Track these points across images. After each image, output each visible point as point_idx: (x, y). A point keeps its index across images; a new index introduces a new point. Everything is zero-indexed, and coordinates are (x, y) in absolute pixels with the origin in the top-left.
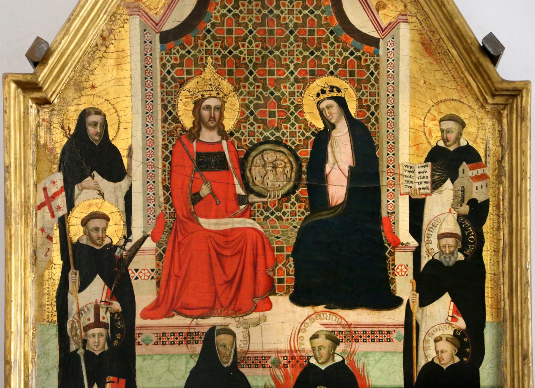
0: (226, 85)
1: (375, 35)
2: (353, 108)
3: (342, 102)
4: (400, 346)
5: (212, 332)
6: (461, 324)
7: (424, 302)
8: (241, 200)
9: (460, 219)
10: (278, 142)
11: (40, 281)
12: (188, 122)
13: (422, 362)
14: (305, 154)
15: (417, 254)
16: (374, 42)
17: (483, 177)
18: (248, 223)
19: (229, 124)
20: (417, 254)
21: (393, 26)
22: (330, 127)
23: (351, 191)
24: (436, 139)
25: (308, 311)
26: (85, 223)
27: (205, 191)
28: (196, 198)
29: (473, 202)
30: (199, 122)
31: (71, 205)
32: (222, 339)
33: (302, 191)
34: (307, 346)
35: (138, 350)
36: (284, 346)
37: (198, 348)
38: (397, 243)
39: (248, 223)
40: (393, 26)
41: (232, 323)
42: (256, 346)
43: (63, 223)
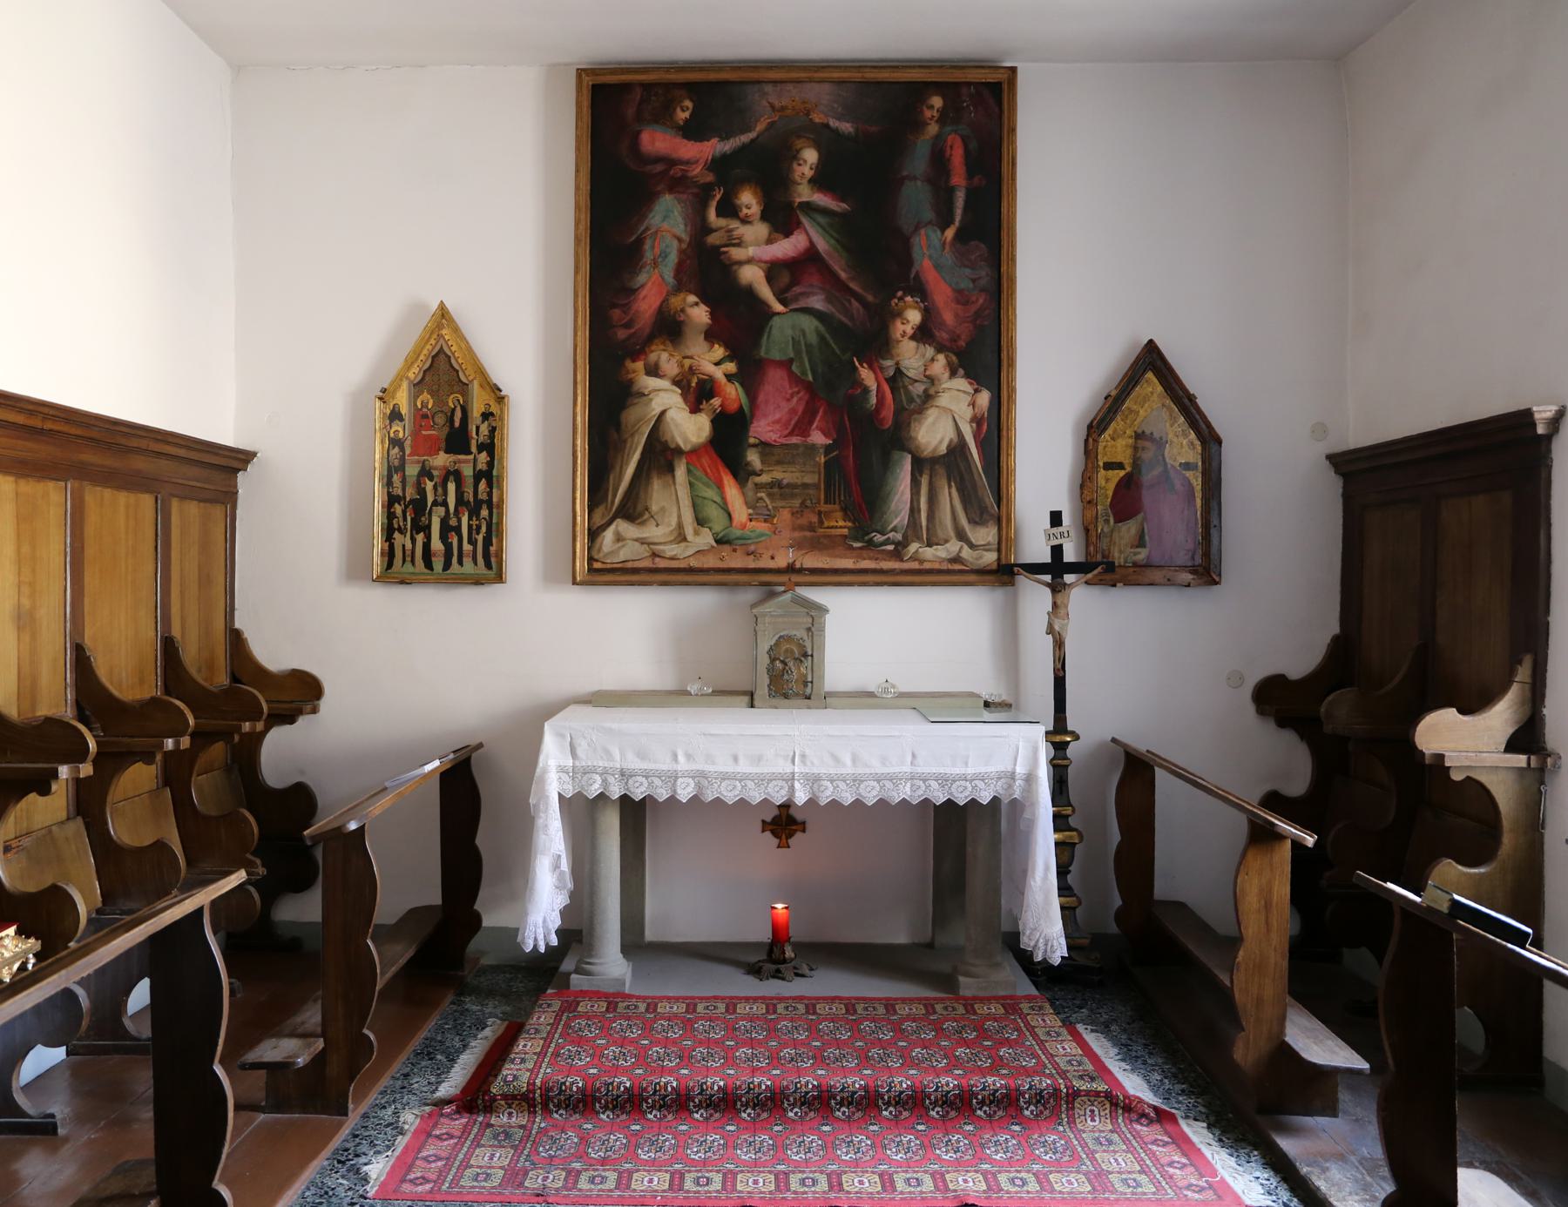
0: (429, 396)
1: (467, 382)
2: (461, 402)
3: (458, 400)
4: (472, 465)
5: (424, 461)
6: (489, 459)
7: (479, 453)
8: (432, 426)
9: (489, 431)
10: (442, 411)
11: (383, 447)
12: (420, 407)
13: (478, 469)
14: (449, 414)
15: (477, 440)
16: (467, 385)
17: (495, 420)
18: (434, 432)
19: (430, 407)
20: (477, 440)
21: (472, 380)
22: (455, 407)
23: (460, 424)
24: (483, 410)
25: (449, 455)
26: (394, 433)
27: (423, 424)
28: (421, 426)
29: (492, 427)
30: (422, 406)
31: (391, 428)
32: (427, 462)
33: (448, 424)
34: (448, 464)
35: (406, 465)
36: (442, 464)
37: (421, 465)
38: (472, 438)
39: (434, 432)
40: (472, 380)
41: (429, 458)
42: (435, 464)
43: (389, 433)
